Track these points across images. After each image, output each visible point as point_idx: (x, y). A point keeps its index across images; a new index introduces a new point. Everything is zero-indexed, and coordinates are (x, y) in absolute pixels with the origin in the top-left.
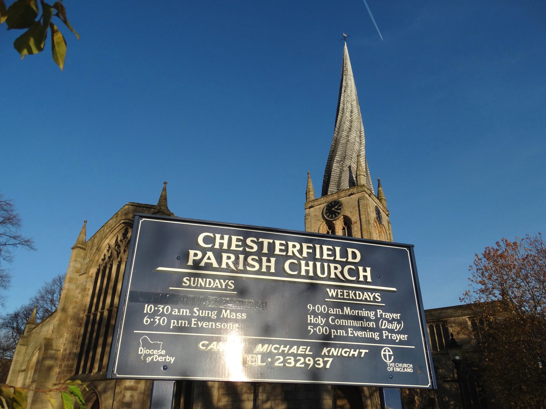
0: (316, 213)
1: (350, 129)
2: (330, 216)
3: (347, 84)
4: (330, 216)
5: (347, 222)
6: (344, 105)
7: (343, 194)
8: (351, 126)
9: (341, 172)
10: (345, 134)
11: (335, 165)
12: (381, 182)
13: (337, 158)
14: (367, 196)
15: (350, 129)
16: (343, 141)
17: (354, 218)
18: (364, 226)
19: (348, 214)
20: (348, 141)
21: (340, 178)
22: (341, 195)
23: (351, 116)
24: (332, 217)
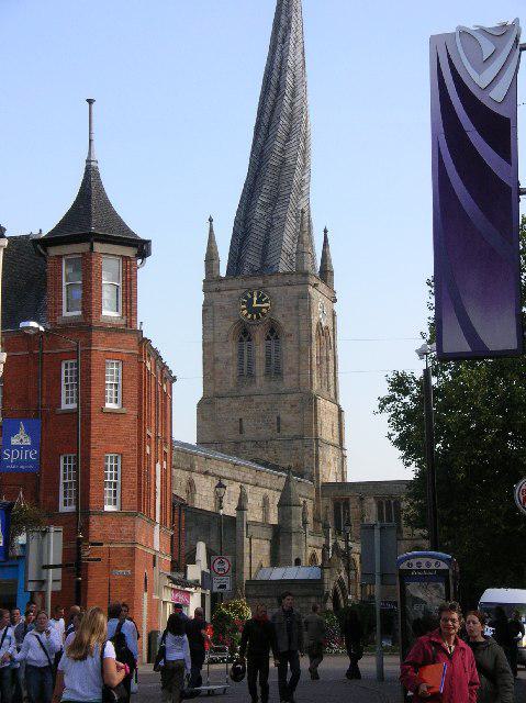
0: (223, 304)
2: (249, 316)
3: (289, 22)
4: (249, 316)
5: (273, 332)
6: (280, 74)
7: (272, 281)
8: (290, 129)
10: (278, 145)
11: (259, 212)
12: (328, 234)
13: (262, 199)
14: (311, 289)
16: (274, 162)
17: (288, 327)
18: (304, 344)
19: (278, 317)
20: (283, 162)
21: (266, 242)
23: (292, 104)
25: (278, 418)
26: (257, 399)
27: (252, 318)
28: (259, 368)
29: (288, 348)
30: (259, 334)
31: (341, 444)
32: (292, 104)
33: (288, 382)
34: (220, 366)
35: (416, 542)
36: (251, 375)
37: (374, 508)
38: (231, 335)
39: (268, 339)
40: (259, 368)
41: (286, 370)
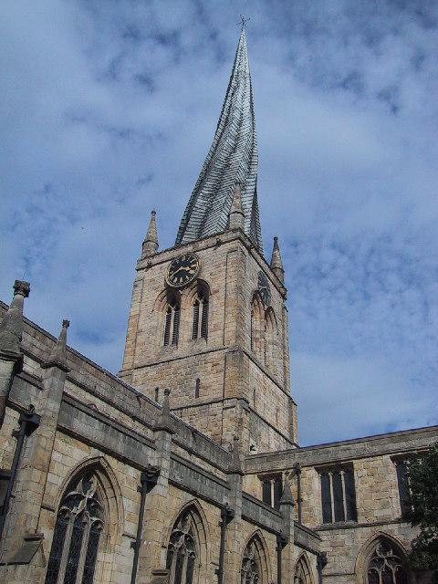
1: (234, 149)
5: (203, 291)
7: (202, 244)
9: (207, 212)
15: (234, 149)
19: (206, 276)
22: (200, 245)
23: (238, 130)
24: (178, 281)
25: (198, 380)
26: (175, 364)
27: (178, 281)
28: (185, 332)
29: (216, 303)
30: (188, 300)
31: (292, 437)
32: (238, 130)
33: (215, 338)
34: (141, 339)
35: (378, 528)
36: (175, 341)
37: (316, 484)
38: (157, 306)
39: (197, 304)
40: (185, 332)
41: (210, 327)
